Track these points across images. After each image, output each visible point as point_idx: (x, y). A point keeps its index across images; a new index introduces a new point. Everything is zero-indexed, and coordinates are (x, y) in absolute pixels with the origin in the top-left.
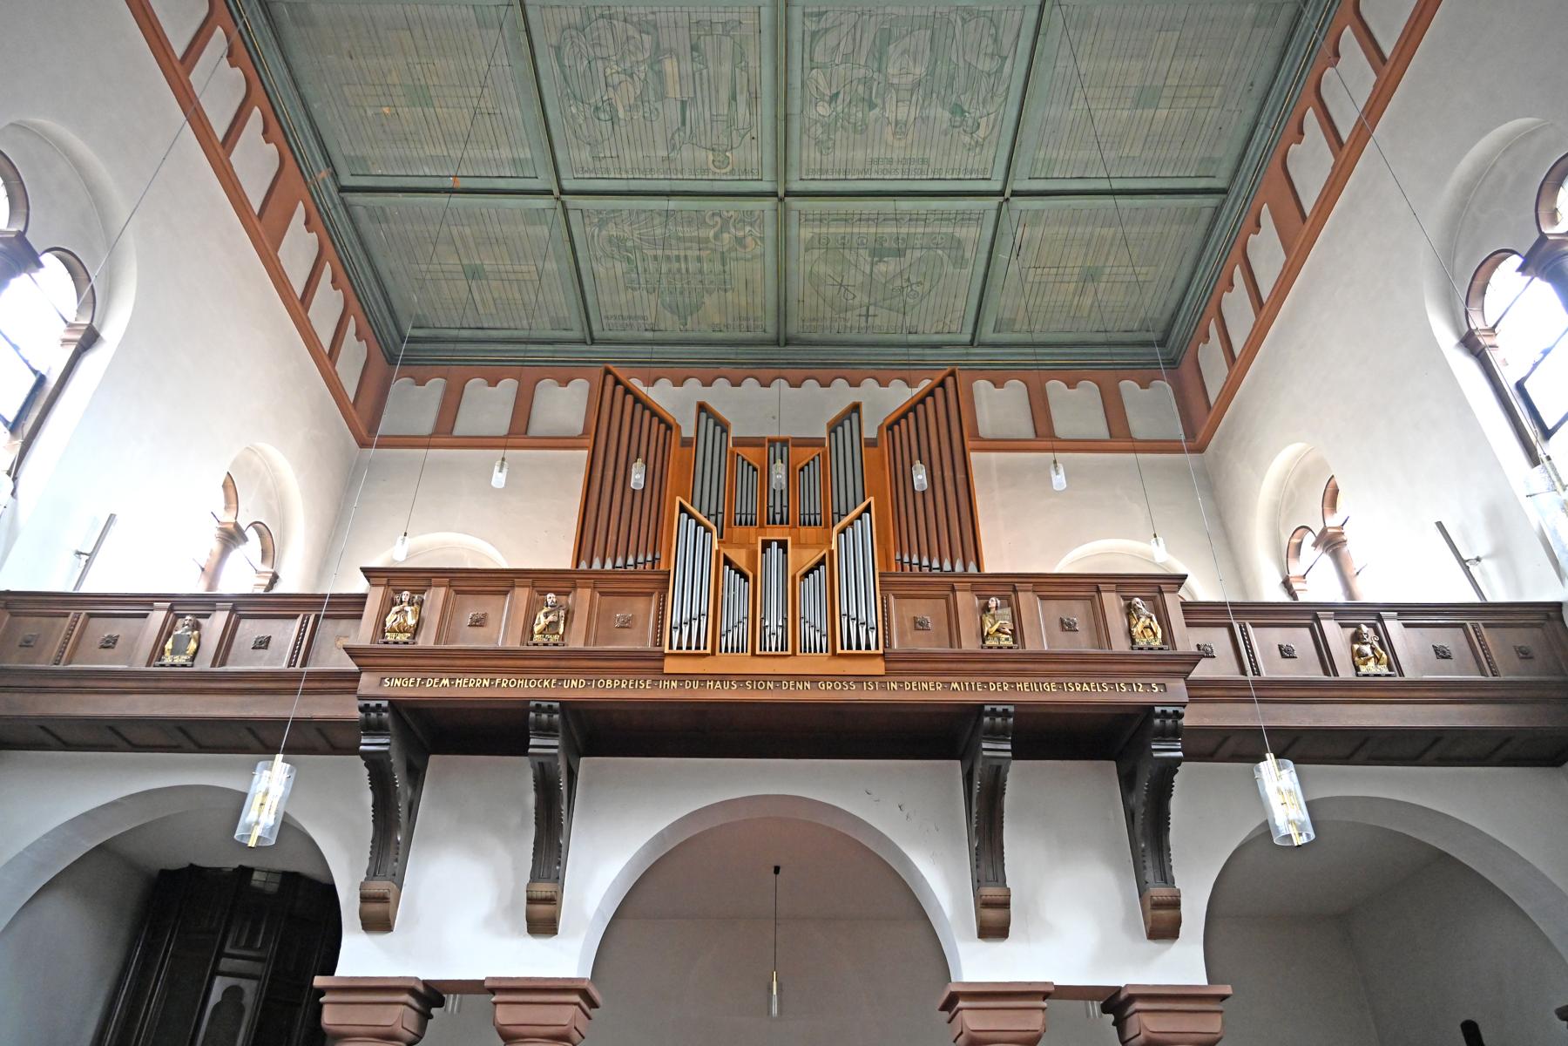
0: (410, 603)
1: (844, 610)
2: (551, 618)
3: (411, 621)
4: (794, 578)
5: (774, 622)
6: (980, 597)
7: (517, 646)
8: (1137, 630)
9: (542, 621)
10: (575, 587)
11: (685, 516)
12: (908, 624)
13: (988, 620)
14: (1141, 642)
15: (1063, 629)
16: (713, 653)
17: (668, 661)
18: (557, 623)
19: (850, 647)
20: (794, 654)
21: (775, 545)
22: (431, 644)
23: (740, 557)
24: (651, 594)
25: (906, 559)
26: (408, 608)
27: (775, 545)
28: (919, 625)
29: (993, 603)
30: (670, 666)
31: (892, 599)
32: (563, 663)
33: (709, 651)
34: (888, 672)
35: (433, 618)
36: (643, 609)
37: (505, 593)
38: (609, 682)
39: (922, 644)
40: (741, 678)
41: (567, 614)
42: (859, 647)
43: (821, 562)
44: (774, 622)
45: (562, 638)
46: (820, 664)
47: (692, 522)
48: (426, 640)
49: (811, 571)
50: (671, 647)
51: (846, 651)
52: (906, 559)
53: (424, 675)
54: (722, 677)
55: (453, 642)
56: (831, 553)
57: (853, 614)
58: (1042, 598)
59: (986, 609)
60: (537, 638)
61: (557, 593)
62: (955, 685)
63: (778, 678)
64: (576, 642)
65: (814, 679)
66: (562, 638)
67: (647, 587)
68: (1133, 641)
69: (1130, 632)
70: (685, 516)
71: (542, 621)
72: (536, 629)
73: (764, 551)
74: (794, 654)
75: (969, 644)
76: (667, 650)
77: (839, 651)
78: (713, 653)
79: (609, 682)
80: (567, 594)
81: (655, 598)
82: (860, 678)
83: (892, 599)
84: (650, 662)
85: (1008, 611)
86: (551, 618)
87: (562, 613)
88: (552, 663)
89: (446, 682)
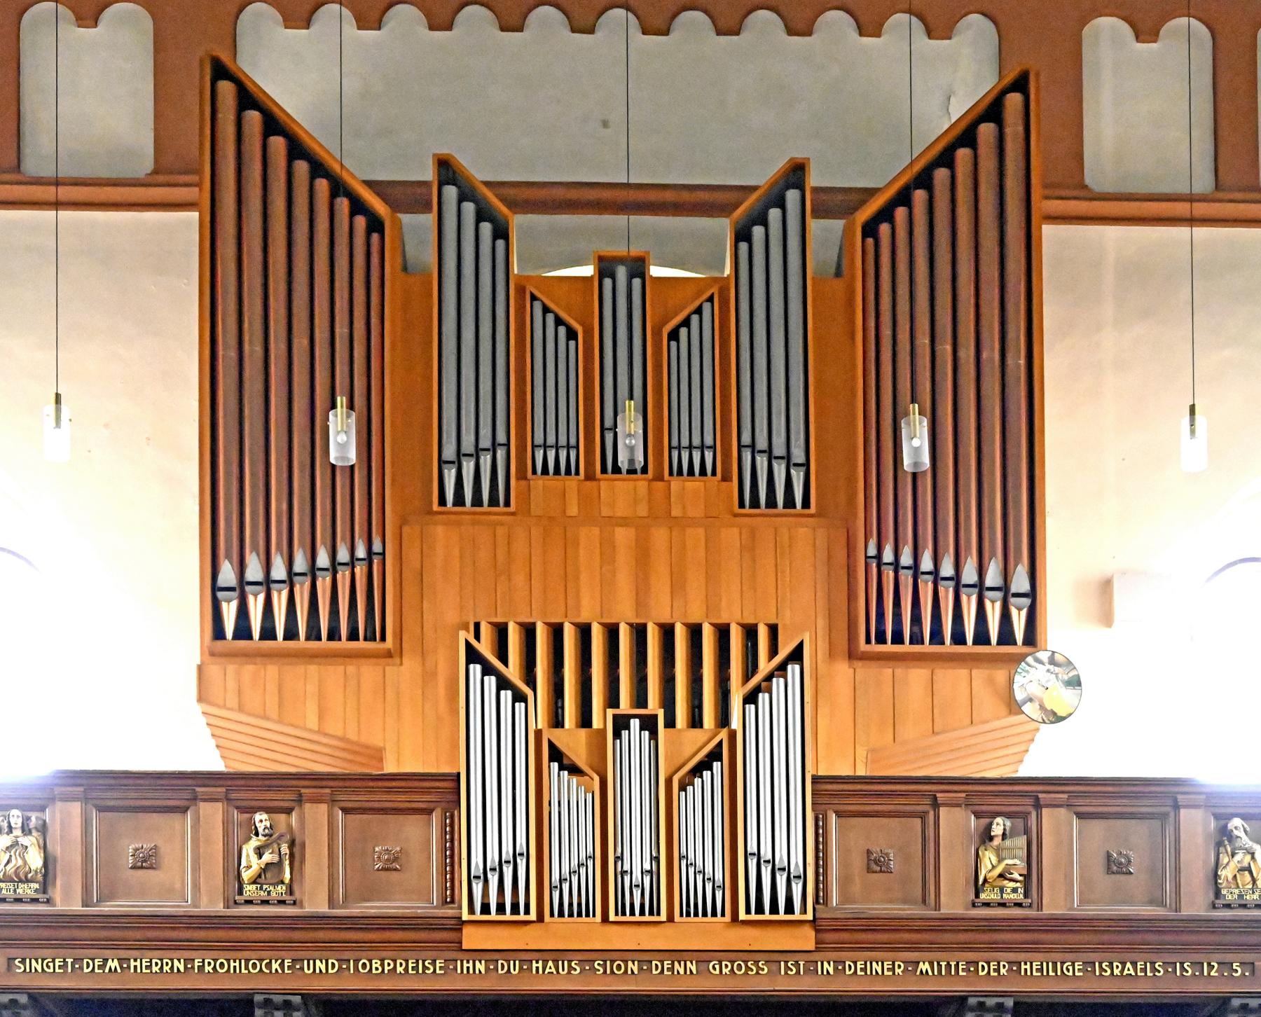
0: (26, 831)
1: (752, 847)
2: (267, 857)
3: (35, 860)
4: (669, 782)
5: (638, 861)
6: (978, 815)
7: (219, 908)
8: (1226, 874)
9: (251, 863)
10: (300, 800)
11: (476, 669)
12: (858, 862)
13: (989, 858)
14: (1230, 895)
15: (1109, 871)
16: (540, 918)
17: (467, 931)
18: (279, 864)
19: (760, 910)
20: (671, 919)
21: (635, 724)
22: (77, 907)
23: (573, 741)
24: (429, 812)
25: (888, 556)
26: (25, 841)
27: (635, 724)
28: (876, 864)
29: (997, 830)
30: (472, 938)
31: (833, 818)
32: (297, 935)
33: (533, 916)
34: (820, 946)
35: (70, 856)
36: (418, 836)
37: (184, 810)
38: (376, 964)
39: (881, 903)
40: (588, 956)
41: (292, 844)
42: (774, 910)
43: (715, 755)
44: (638, 861)
45: (291, 891)
46: (710, 933)
47: (491, 681)
48: (67, 900)
49: (697, 770)
50: (471, 910)
51: (753, 917)
52: (888, 556)
53: (79, 953)
54: (558, 955)
55: (112, 897)
56: (732, 735)
57: (766, 853)
58: (1080, 816)
59: (987, 837)
60: (250, 890)
61: (268, 810)
62: (924, 967)
63: (644, 956)
64: (316, 904)
65: (703, 957)
66: (291, 891)
67: (420, 801)
68: (1218, 893)
69: (1216, 876)
70: (476, 669)
71: (251, 863)
72: (246, 875)
73: (617, 735)
74: (671, 919)
75: (953, 902)
76: (465, 917)
77: (742, 916)
78: (540, 918)
79: (376, 964)
80: (288, 811)
81: (436, 817)
82: (774, 956)
83: (833, 818)
84: (442, 933)
85: (1021, 841)
86: (267, 857)
87: (285, 849)
88: (280, 935)
89: (113, 964)
